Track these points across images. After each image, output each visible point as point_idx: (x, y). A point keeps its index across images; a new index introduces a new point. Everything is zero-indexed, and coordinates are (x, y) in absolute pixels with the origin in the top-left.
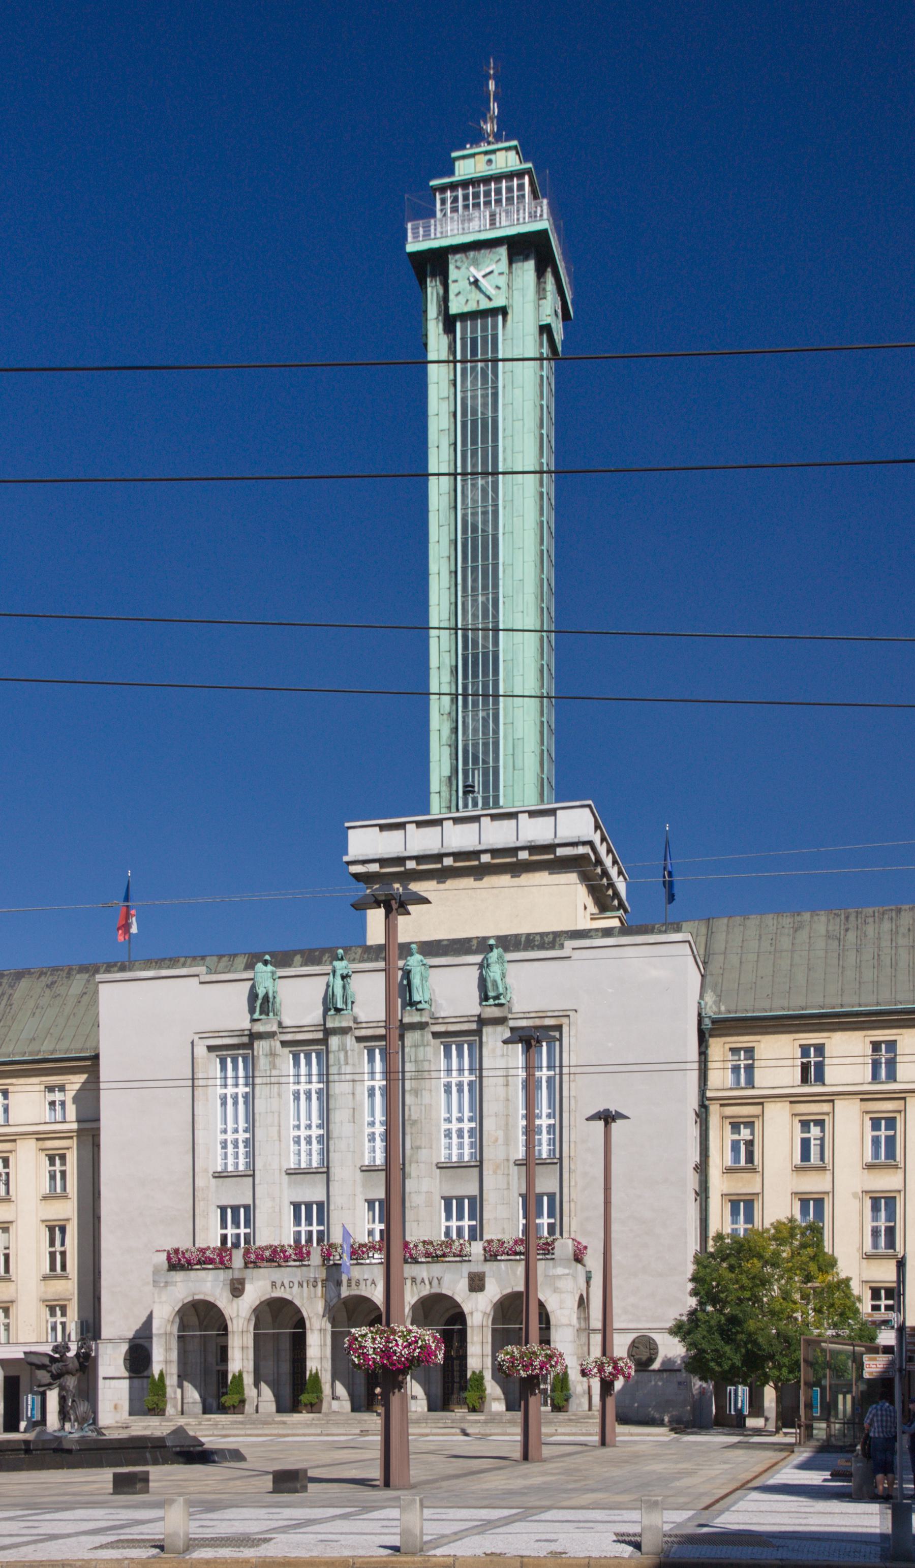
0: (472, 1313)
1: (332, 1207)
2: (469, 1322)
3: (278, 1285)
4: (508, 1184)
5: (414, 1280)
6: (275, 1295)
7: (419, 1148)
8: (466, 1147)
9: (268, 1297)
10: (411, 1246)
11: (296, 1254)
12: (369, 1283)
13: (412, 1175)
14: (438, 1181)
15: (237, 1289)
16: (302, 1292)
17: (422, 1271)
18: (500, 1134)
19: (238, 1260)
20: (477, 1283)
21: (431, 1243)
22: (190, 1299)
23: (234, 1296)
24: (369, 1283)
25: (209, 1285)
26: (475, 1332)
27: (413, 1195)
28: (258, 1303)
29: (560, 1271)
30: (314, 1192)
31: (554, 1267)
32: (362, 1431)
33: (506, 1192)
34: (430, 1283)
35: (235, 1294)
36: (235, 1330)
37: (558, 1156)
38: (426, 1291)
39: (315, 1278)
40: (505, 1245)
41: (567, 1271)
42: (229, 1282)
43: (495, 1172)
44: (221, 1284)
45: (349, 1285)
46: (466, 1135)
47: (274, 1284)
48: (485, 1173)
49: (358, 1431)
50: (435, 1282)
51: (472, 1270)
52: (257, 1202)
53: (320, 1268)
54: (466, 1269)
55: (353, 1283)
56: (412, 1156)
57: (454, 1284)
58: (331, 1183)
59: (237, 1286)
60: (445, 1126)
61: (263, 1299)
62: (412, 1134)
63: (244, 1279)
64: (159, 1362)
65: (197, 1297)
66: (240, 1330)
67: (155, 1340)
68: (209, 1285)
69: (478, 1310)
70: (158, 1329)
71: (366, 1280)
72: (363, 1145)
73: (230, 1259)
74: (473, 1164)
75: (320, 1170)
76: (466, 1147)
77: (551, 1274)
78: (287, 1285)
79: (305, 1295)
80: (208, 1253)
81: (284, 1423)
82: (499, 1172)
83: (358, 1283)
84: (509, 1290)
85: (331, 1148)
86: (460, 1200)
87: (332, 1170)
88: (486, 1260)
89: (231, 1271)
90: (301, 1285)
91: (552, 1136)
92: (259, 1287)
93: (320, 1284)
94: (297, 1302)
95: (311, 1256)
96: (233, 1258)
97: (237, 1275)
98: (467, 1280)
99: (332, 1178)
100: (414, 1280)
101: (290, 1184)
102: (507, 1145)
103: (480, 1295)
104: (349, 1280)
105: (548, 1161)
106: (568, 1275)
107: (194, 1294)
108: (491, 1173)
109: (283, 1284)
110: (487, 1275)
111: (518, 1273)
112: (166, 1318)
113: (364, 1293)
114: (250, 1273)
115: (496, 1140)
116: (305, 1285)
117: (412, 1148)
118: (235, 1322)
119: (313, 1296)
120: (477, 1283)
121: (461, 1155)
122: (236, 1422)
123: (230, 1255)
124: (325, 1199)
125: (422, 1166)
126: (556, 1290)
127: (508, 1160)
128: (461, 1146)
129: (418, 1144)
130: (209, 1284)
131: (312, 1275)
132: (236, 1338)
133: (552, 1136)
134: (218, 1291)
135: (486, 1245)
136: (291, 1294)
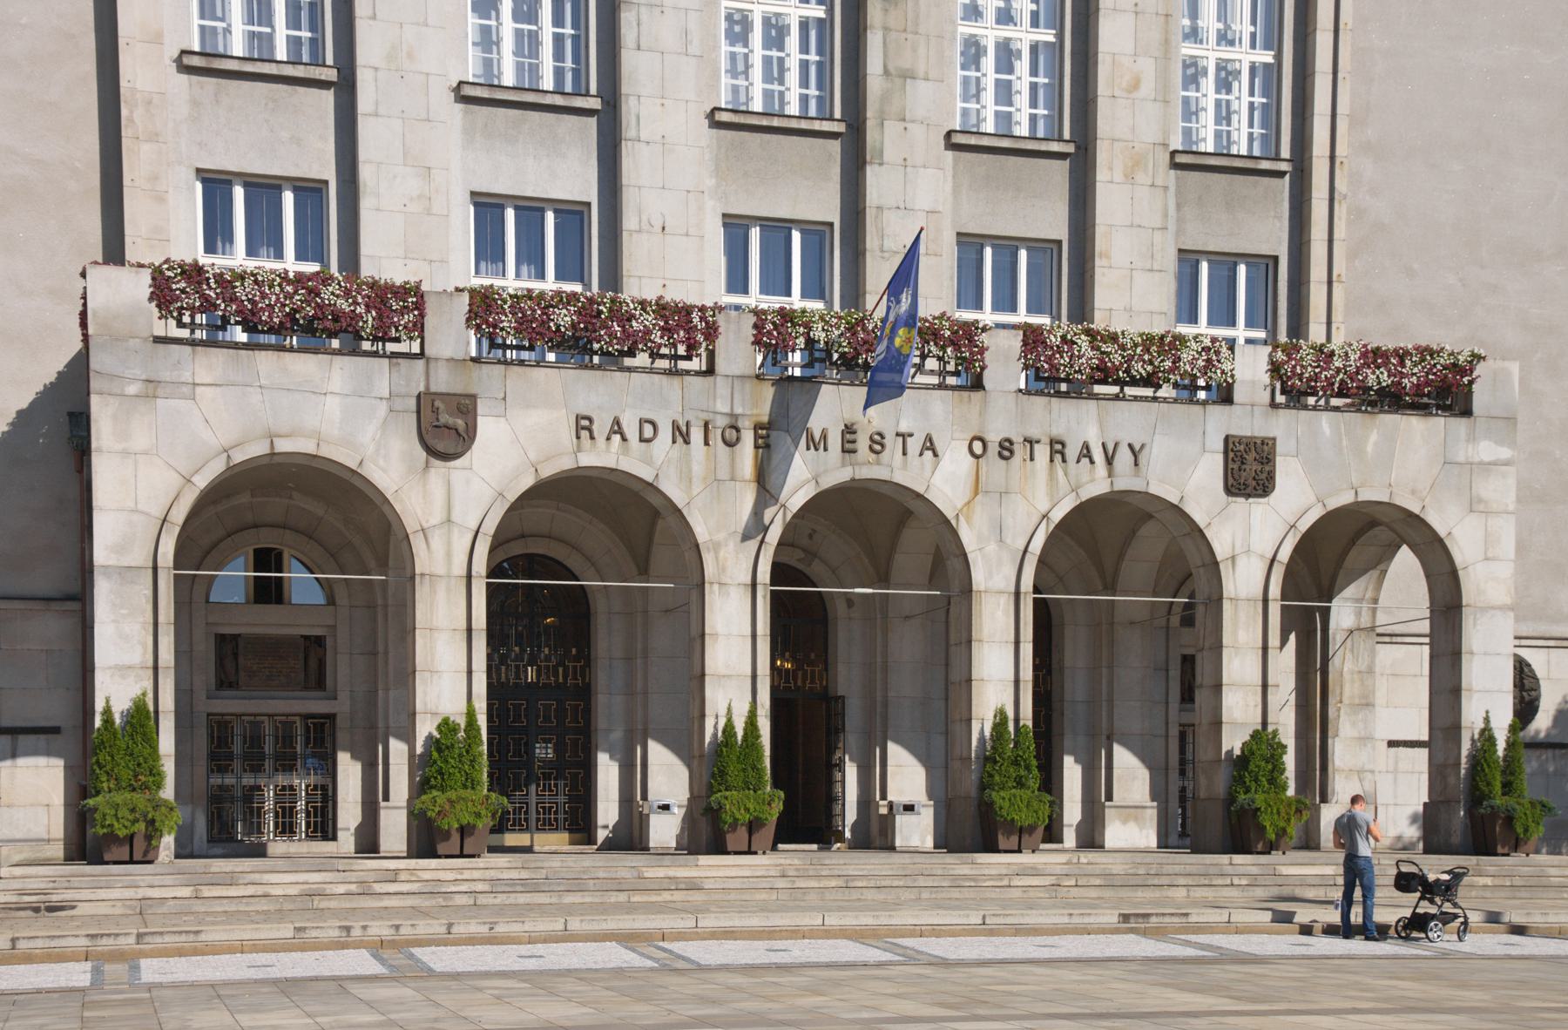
0: (1233, 558)
1: (629, 221)
2: (1229, 588)
3: (601, 427)
4: (1166, 215)
5: (1057, 448)
6: (587, 460)
7: (907, 75)
8: (1022, 100)
9: (566, 464)
10: (1054, 340)
11: (667, 330)
12: (914, 445)
13: (887, 156)
14: (949, 187)
15: (444, 430)
16: (686, 460)
17: (1082, 421)
18: (1147, 67)
19: (450, 334)
20: (1249, 470)
21: (1113, 338)
22: (258, 449)
23: (432, 452)
24: (914, 445)
25: (335, 410)
26: (1242, 616)
27: (890, 217)
28: (528, 482)
29: (1487, 450)
30: (562, 169)
31: (1472, 438)
32: (1125, 918)
33: (1158, 235)
34: (1109, 461)
35: (440, 447)
36: (441, 571)
37: (1285, 152)
38: (1096, 484)
39: (733, 415)
40: (1338, 363)
41: (1505, 453)
42: (413, 403)
43: (1130, 178)
44: (383, 408)
45: (848, 449)
46: (1023, 65)
47: (584, 425)
48: (1102, 175)
49: (1111, 918)
50: (1124, 457)
51: (1236, 431)
52: (366, 173)
53: (748, 385)
54: (1219, 423)
55: (863, 444)
56: (885, 98)
57: (1179, 462)
58: (626, 149)
59: (445, 418)
60: (966, 29)
61: (547, 471)
62: (886, 29)
63: (473, 397)
64: (123, 670)
65: (284, 446)
66: (460, 568)
67: (103, 591)
68: (335, 410)
69: (1250, 545)
70: (120, 549)
71: (904, 436)
72: (716, 47)
73: (418, 328)
74: (1055, 147)
75: (579, 102)
76: (1022, 100)
77: (1461, 458)
78: (631, 431)
79: (698, 468)
80: (327, 294)
81: (693, 886)
82: (1141, 177)
83: (877, 443)
84: (1346, 498)
85: (628, 34)
86: (1007, 247)
87: (630, 108)
88: (1274, 405)
89: (420, 363)
90: (681, 434)
91: (1259, 100)
92: (531, 429)
93: (748, 438)
94: (673, 490)
95: (720, 342)
96: (429, 322)
97: (443, 381)
98: (1220, 458)
99: (629, 129)
100: (1057, 448)
101: (469, 132)
102: (1166, 102)
103: (1257, 507)
104: (849, 430)
105: (1265, 165)
106: (1507, 463)
107: (271, 437)
108: (1118, 176)
109: (617, 428)
110: (1278, 449)
111: (1369, 448)
112: (159, 513)
113: (900, 478)
114: (488, 381)
115: (1135, 85)
116: (697, 435)
117: (886, 72)
118: (437, 542)
119: (723, 473)
120: (1249, 470)
121: (1005, 119)
122: (513, 886)
123: (420, 306)
124: (592, 196)
125: (916, 130)
126: (1474, 505)
127: (1165, 145)
128: (1005, 92)
129: (905, 63)
130: (333, 405)
131: (722, 406)
132: (441, 594)
133: (1259, 100)
134: (368, 434)
135: (1280, 356)
136: (648, 461)
